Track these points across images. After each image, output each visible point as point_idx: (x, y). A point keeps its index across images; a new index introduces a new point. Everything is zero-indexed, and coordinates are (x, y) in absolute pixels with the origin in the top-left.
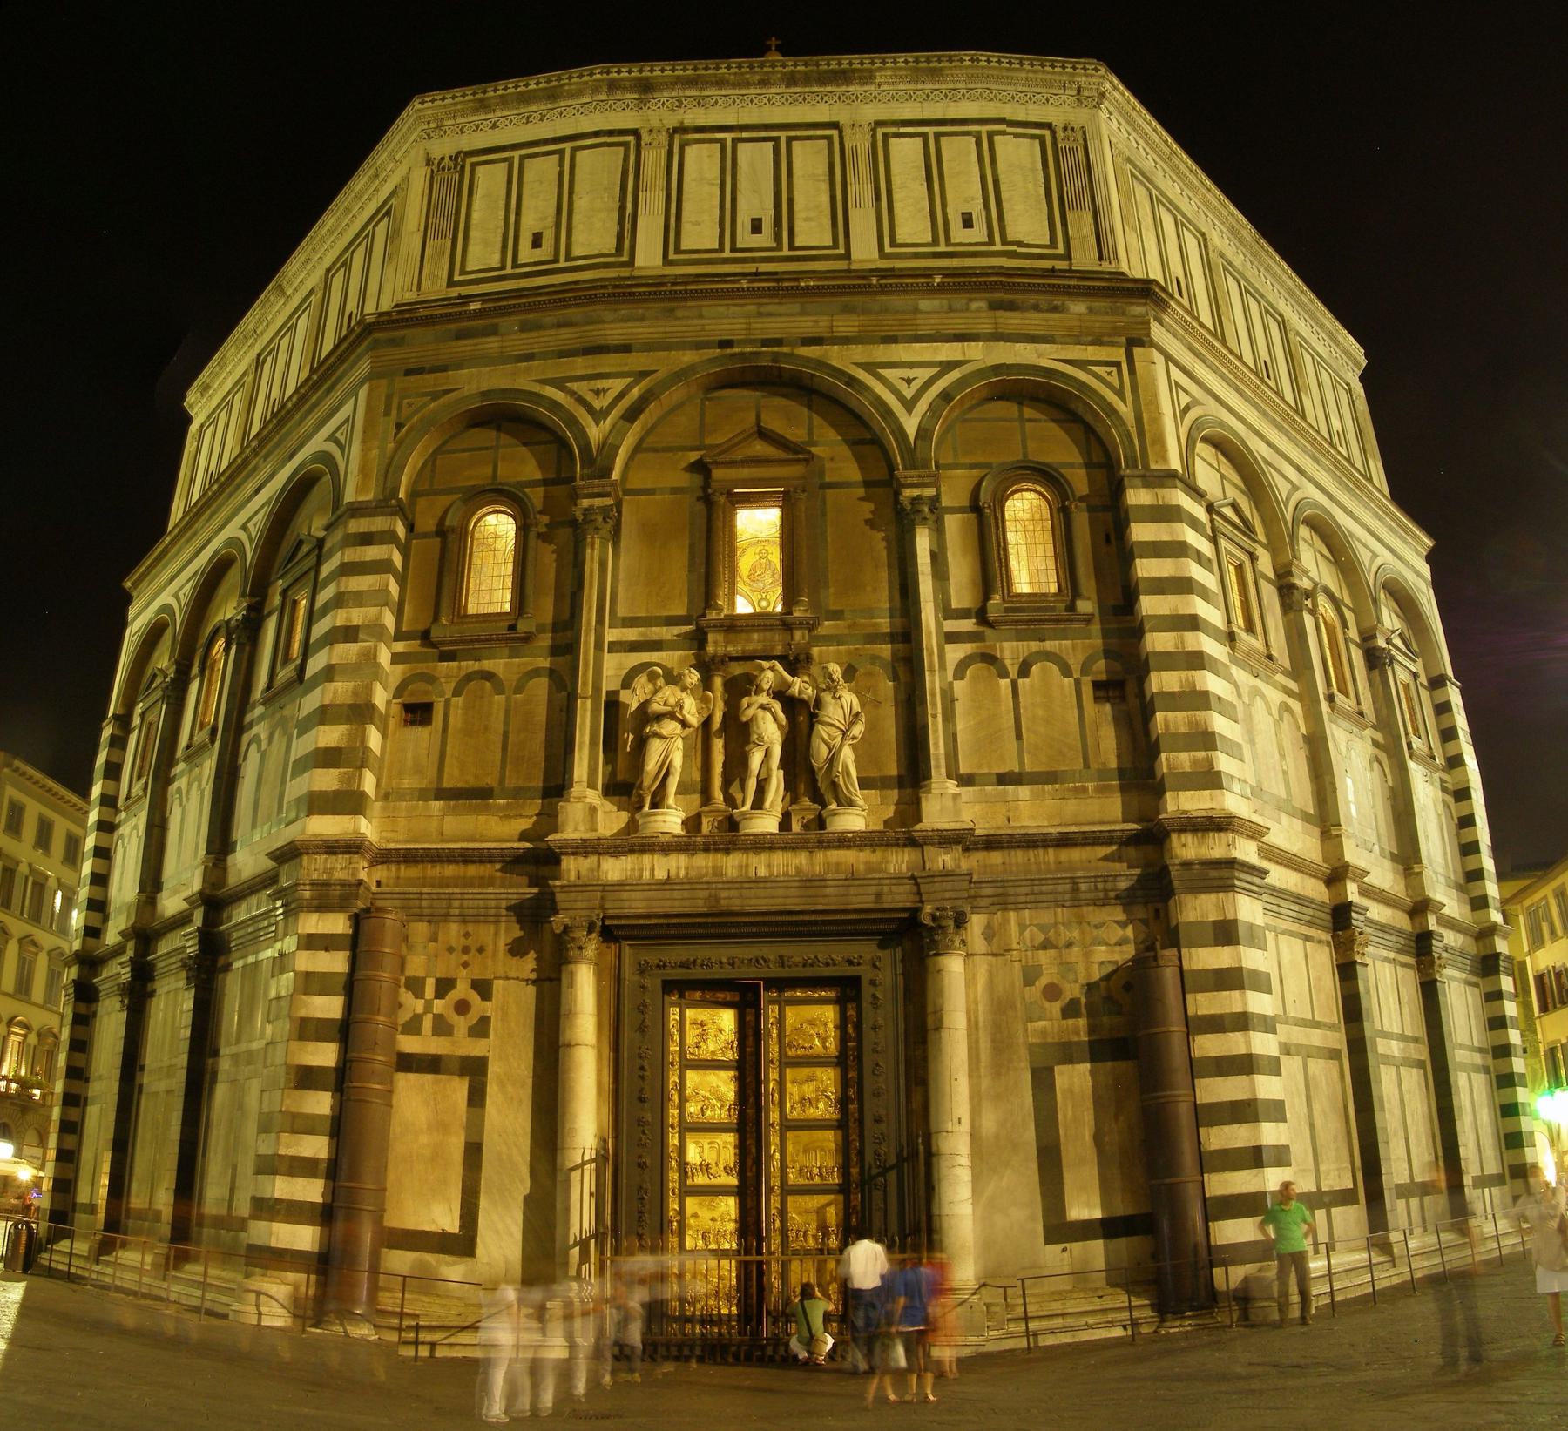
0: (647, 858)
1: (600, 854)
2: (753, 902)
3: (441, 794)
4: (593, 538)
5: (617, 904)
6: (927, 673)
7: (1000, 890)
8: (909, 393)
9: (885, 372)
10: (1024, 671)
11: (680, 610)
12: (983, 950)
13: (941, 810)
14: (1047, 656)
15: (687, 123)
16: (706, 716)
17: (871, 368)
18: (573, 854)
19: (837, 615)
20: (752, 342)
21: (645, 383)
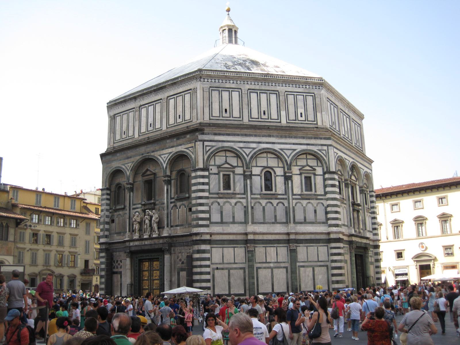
0: (135, 242)
3: (116, 233)
8: (165, 160)
9: (162, 156)
10: (180, 208)
11: (140, 202)
14: (183, 204)
15: (142, 104)
17: (160, 155)
19: (158, 200)
20: (145, 153)
21: (133, 163)
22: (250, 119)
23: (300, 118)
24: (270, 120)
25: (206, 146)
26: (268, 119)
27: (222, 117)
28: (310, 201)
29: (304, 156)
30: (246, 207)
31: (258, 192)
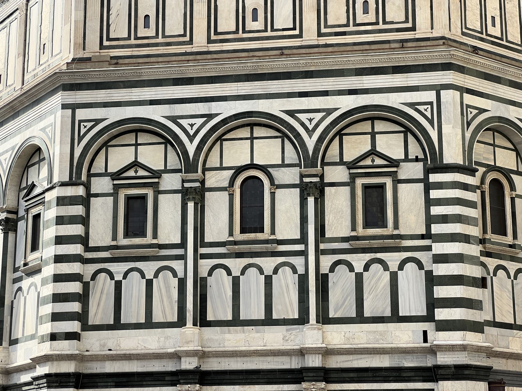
22: (213, 37)
23: (361, 18)
24: (269, 33)
25: (80, 121)
26: (266, 30)
27: (136, 38)
28: (379, 255)
29: (366, 127)
30: (182, 283)
31: (224, 237)
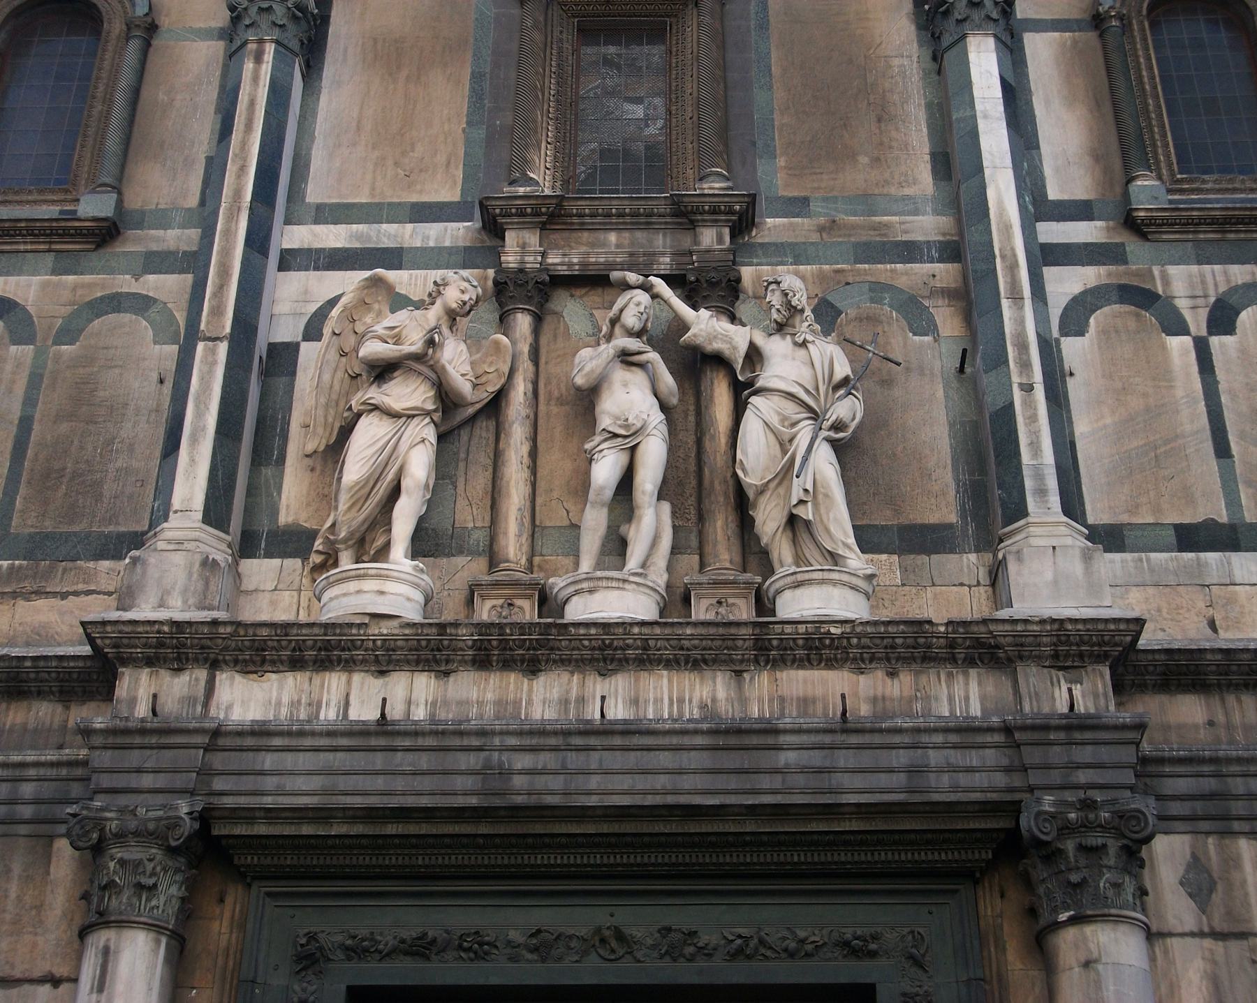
0: (334, 682)
1: (214, 665)
2: (594, 782)
4: (261, 42)
5: (248, 783)
6: (1005, 304)
7: (1209, 784)
11: (449, 192)
12: (1190, 924)
13: (1055, 582)
16: (493, 388)
18: (151, 662)
